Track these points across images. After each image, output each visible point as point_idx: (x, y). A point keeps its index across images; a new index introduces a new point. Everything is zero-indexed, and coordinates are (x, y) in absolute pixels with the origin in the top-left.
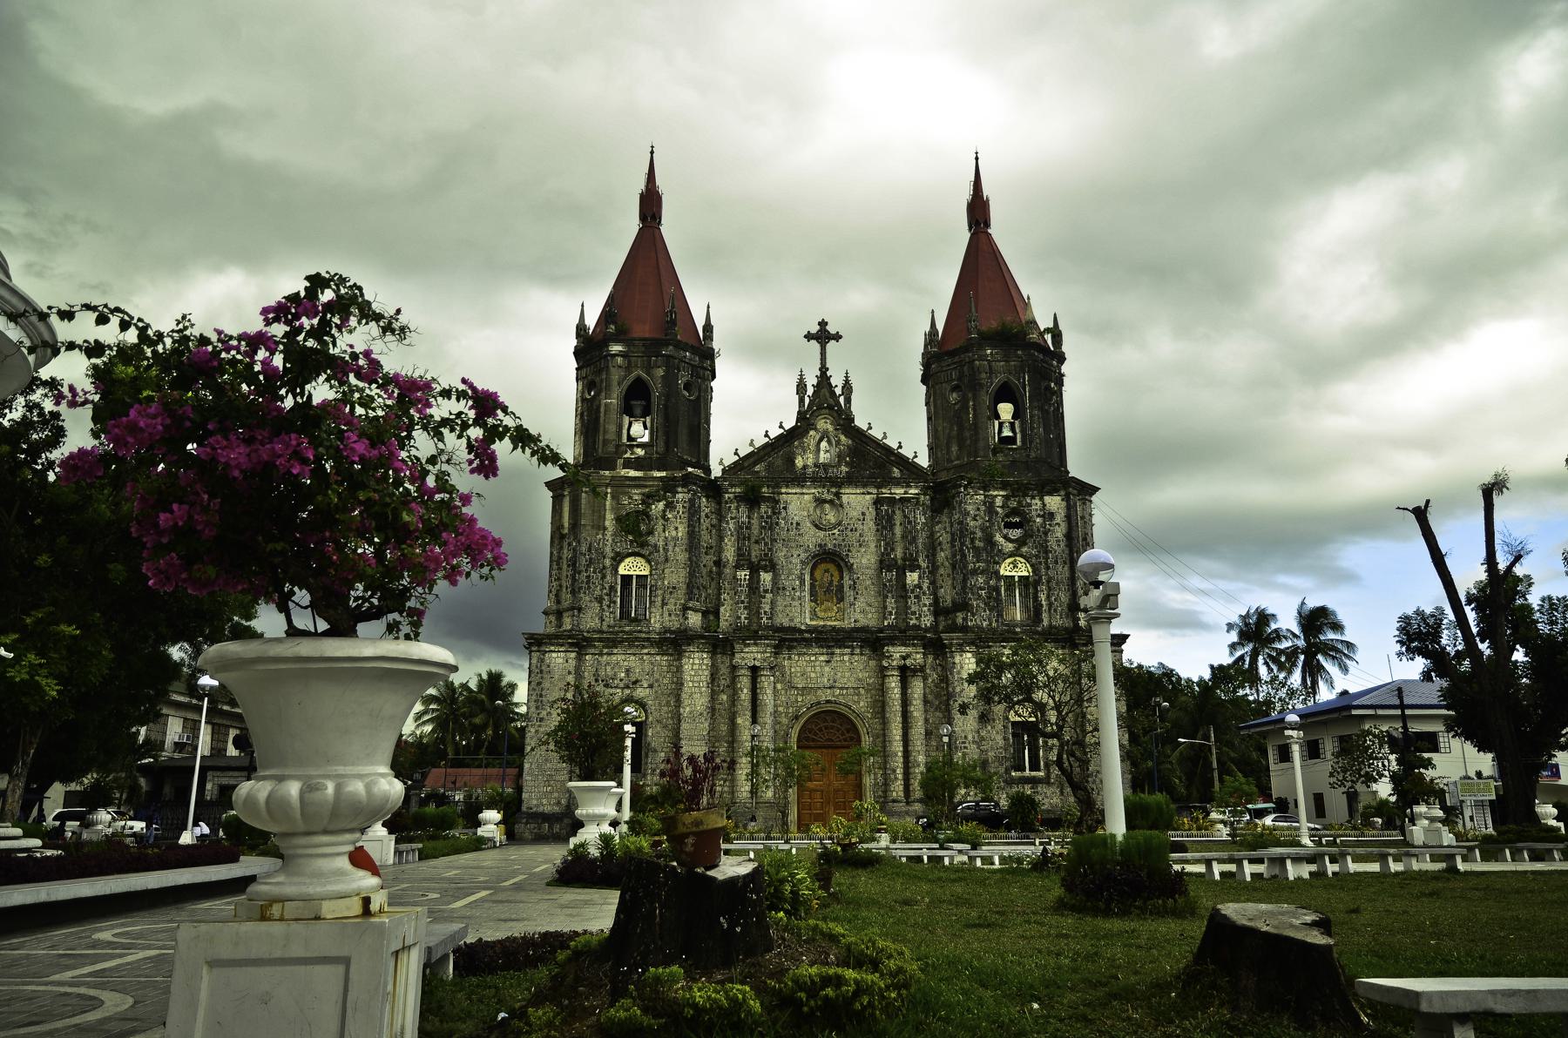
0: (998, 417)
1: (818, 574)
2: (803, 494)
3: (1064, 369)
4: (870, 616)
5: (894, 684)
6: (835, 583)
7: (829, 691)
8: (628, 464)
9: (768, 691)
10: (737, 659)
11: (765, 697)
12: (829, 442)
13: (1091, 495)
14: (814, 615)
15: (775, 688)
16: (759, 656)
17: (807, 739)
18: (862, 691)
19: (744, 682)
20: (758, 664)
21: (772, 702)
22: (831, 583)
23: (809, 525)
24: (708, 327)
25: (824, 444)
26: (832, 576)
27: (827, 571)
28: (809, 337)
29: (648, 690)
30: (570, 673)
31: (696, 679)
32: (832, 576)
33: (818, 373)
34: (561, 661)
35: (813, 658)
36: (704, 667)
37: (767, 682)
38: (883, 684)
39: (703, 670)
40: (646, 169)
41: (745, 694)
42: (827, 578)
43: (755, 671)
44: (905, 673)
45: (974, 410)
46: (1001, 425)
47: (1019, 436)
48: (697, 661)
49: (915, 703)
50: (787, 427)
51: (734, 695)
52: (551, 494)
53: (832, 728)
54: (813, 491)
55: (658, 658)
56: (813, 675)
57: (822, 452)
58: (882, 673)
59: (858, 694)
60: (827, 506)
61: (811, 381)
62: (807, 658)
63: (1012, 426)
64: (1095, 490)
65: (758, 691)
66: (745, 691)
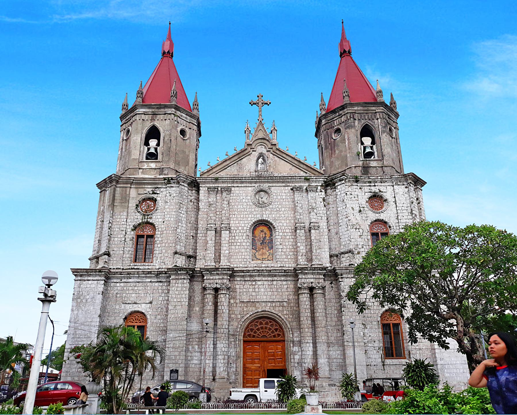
0: (362, 143)
1: (257, 232)
2: (246, 186)
3: (398, 121)
4: (289, 257)
5: (305, 298)
6: (267, 238)
7: (264, 304)
8: (144, 171)
9: (225, 304)
10: (206, 283)
11: (223, 308)
12: (263, 159)
13: (422, 186)
14: (254, 257)
15: (229, 302)
16: (220, 282)
17: (249, 335)
18: (285, 304)
19: (210, 298)
20: (219, 286)
21: (228, 311)
22: (265, 237)
23: (251, 204)
24: (196, 104)
25: (260, 160)
26: (265, 234)
27: (262, 231)
28: (252, 104)
29: (149, 304)
30: (99, 294)
31: (179, 297)
32: (265, 234)
33: (258, 122)
34: (93, 286)
35: (254, 283)
36: (185, 289)
37: (223, 299)
38: (298, 299)
39: (184, 291)
40: (167, 33)
41: (210, 306)
42: (262, 235)
43: (216, 290)
44: (311, 289)
45: (348, 139)
46: (365, 148)
47: (376, 154)
48: (180, 285)
49: (319, 311)
50: (239, 150)
51: (204, 307)
52: (100, 191)
53: (266, 328)
54: (254, 185)
55: (157, 284)
56: (254, 294)
57: (259, 165)
58: (297, 290)
59: (283, 306)
60: (262, 193)
61: (253, 126)
62: (250, 283)
63: (372, 148)
64: (423, 183)
65: (219, 304)
66: (210, 304)
